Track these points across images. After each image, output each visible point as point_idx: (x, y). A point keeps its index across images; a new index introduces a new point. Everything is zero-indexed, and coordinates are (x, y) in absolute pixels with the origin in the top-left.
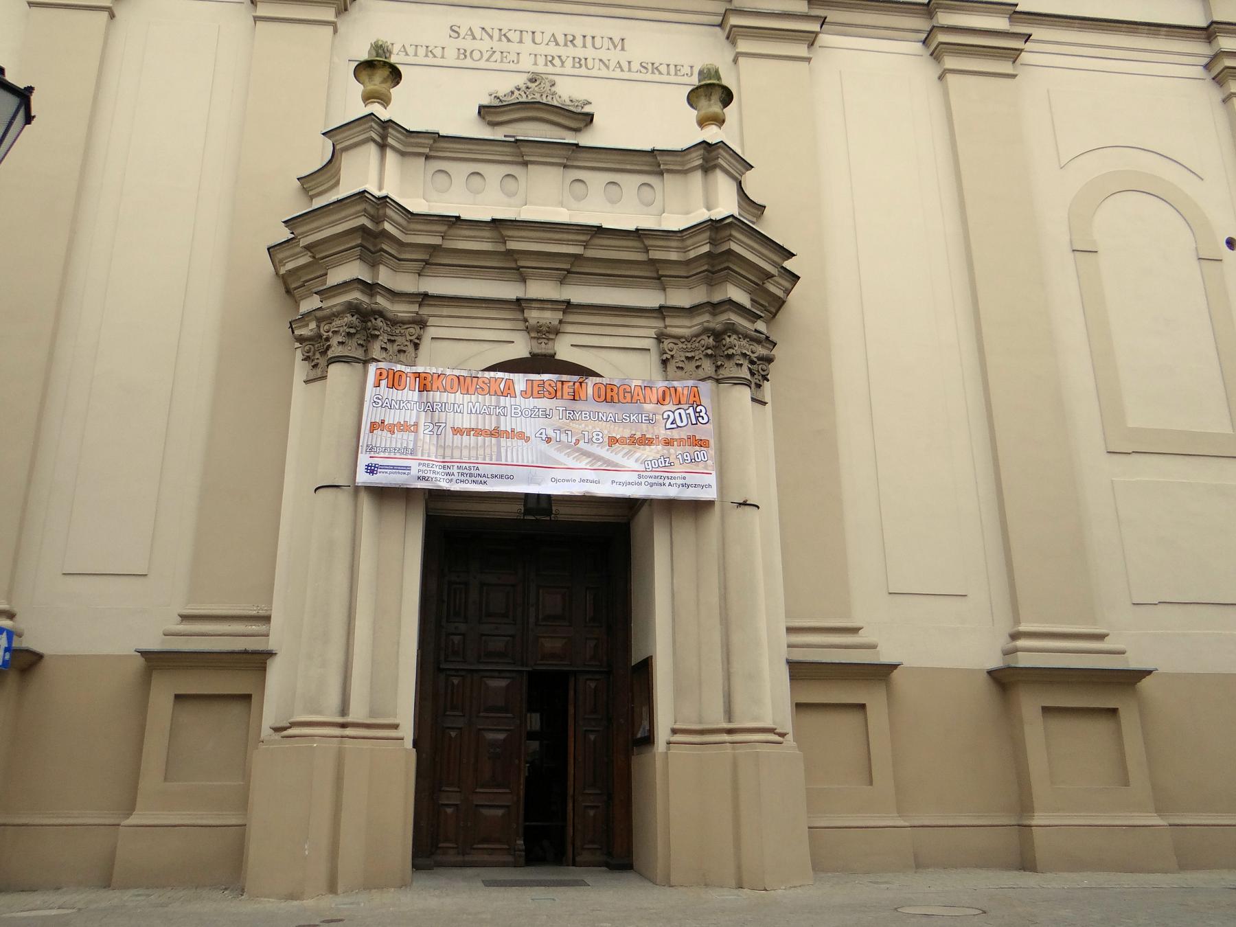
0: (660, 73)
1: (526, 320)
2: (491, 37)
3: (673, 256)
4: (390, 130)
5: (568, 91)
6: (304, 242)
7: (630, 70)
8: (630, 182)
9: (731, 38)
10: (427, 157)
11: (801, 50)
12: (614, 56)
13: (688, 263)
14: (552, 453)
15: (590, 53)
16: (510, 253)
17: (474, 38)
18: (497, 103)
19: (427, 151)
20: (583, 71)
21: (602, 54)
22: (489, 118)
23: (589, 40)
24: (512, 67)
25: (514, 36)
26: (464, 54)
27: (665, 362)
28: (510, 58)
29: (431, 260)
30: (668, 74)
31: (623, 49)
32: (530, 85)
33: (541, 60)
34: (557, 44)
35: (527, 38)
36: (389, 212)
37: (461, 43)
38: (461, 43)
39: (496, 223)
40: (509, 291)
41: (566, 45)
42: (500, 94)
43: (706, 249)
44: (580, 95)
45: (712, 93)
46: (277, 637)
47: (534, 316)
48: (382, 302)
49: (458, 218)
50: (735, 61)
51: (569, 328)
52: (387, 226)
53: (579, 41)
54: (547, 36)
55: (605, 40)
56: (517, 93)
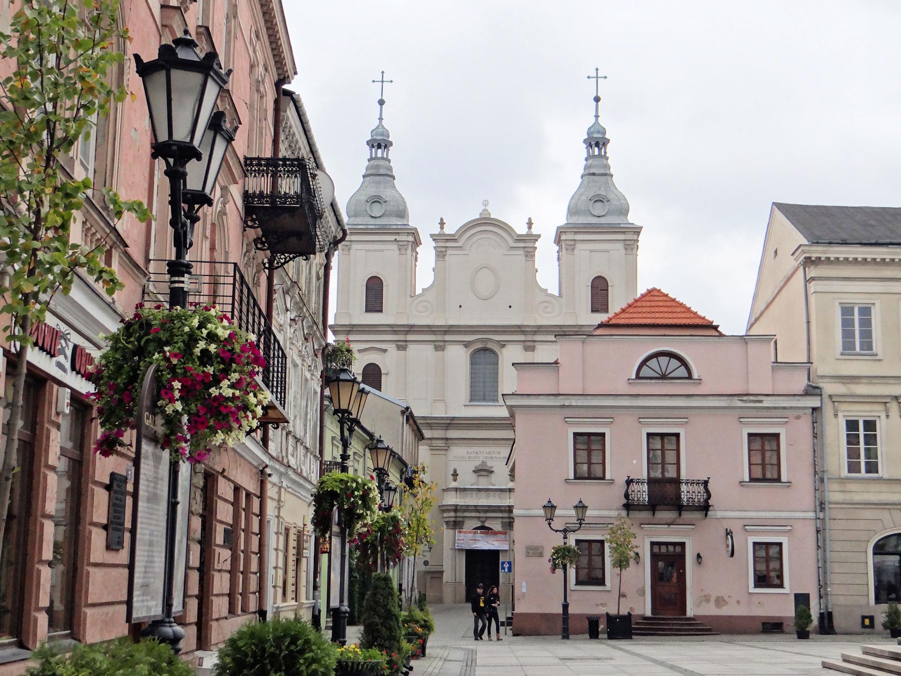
5: (489, 464)
14: (485, 544)
29: (465, 511)
40: (477, 515)
46: (444, 568)
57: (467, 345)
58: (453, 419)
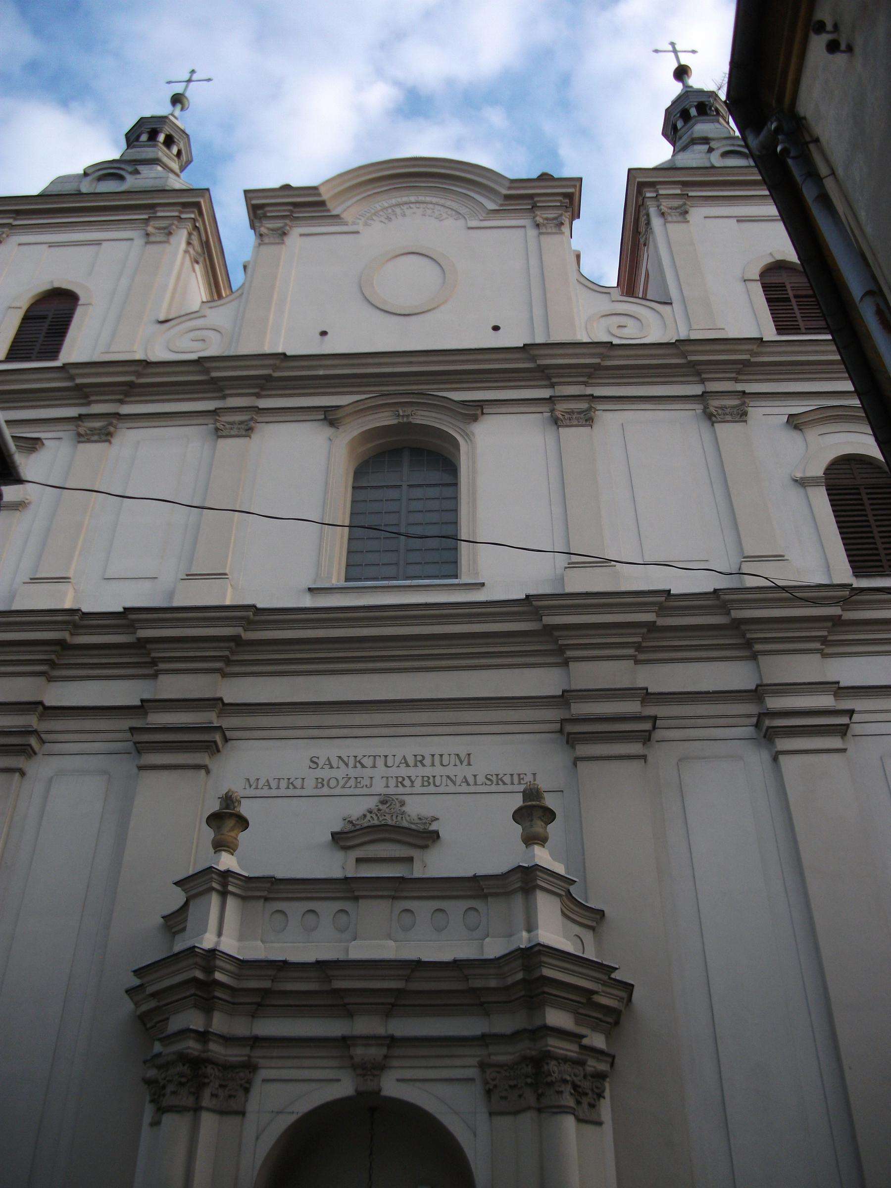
0: (504, 784)
1: (352, 1057)
2: (347, 765)
3: (493, 983)
4: (230, 879)
5: (417, 808)
6: (151, 989)
7: (476, 784)
8: (456, 908)
9: (571, 740)
10: (266, 899)
11: (635, 748)
12: (461, 771)
13: (507, 988)
15: (438, 771)
16: (336, 992)
17: (332, 767)
18: (350, 827)
19: (264, 894)
20: (432, 789)
21: (450, 771)
22: (342, 844)
23: (437, 758)
24: (365, 791)
25: (368, 762)
26: (320, 783)
27: (489, 1092)
28: (364, 783)
29: (262, 1002)
30: (512, 784)
31: (469, 764)
32: (381, 807)
33: (392, 783)
34: (408, 766)
35: (380, 762)
36: (218, 963)
37: (319, 773)
38: (319, 773)
39: (320, 965)
40: (334, 1028)
41: (416, 765)
42: (354, 818)
43: (520, 976)
44: (427, 812)
45: (533, 813)
47: (359, 1052)
48: (216, 1049)
49: (285, 962)
50: (575, 765)
51: (395, 1063)
52: (218, 976)
53: (428, 761)
54: (398, 759)
55: (453, 757)
56: (369, 816)
57: (330, 417)
58: (251, 615)
